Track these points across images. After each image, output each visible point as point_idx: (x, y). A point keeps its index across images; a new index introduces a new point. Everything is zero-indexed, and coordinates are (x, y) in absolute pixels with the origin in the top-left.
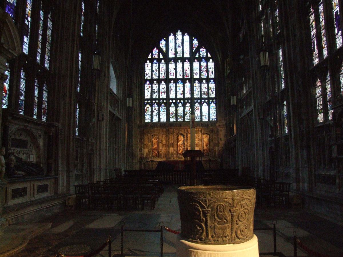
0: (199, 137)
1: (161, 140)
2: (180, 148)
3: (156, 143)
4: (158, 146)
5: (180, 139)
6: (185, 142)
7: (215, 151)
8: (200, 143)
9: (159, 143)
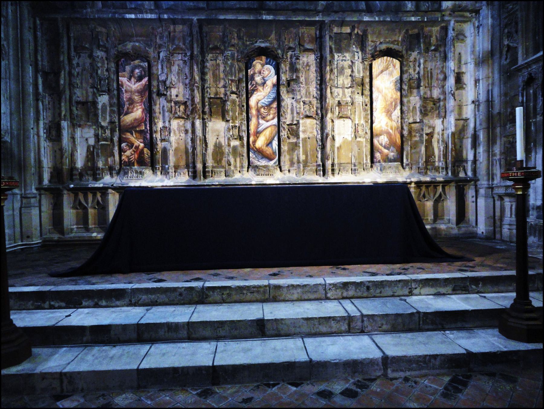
0: (351, 67)
1: (164, 82)
2: (259, 124)
3: (136, 98)
4: (149, 111)
5: (258, 79)
6: (287, 100)
7: (430, 135)
8: (359, 99)
9: (154, 96)
